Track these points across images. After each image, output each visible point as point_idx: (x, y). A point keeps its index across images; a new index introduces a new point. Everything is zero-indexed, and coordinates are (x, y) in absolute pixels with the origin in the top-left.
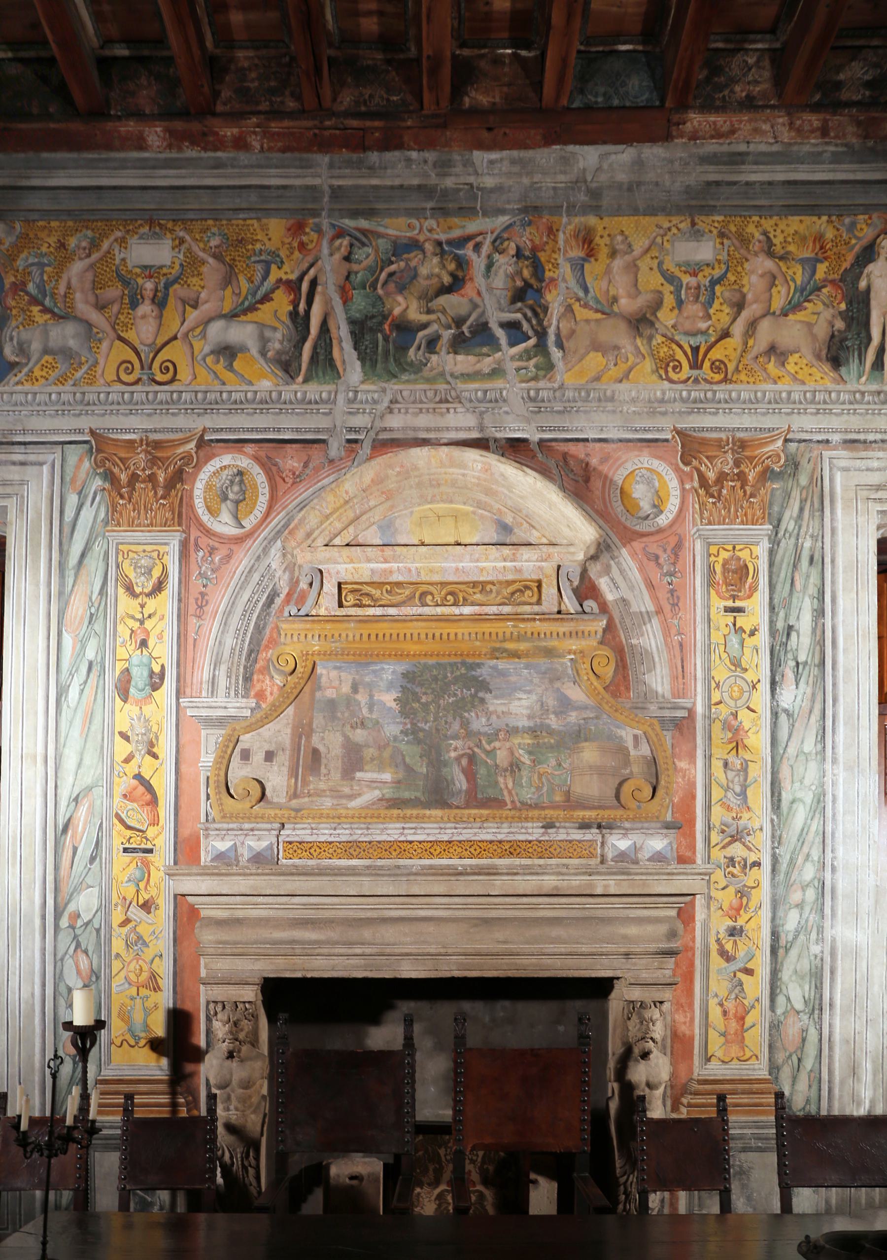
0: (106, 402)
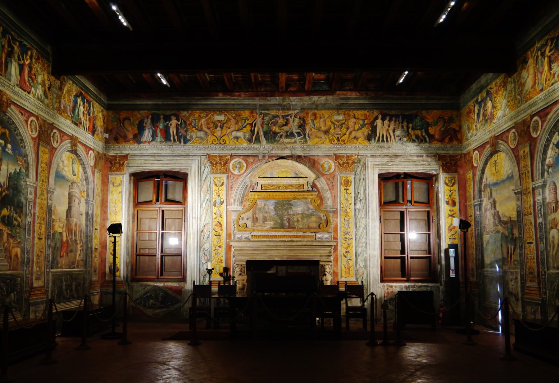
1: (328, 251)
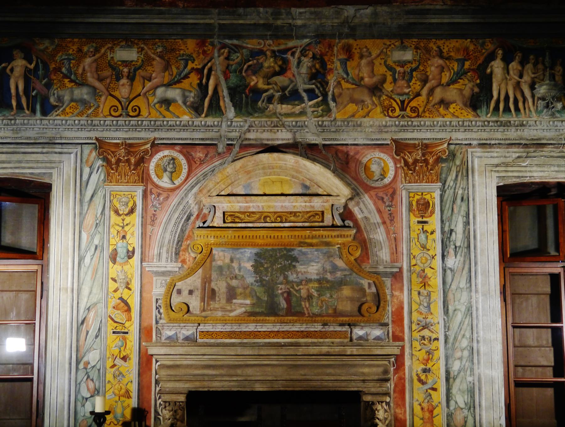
0: (104, 125)
1: (380, 370)
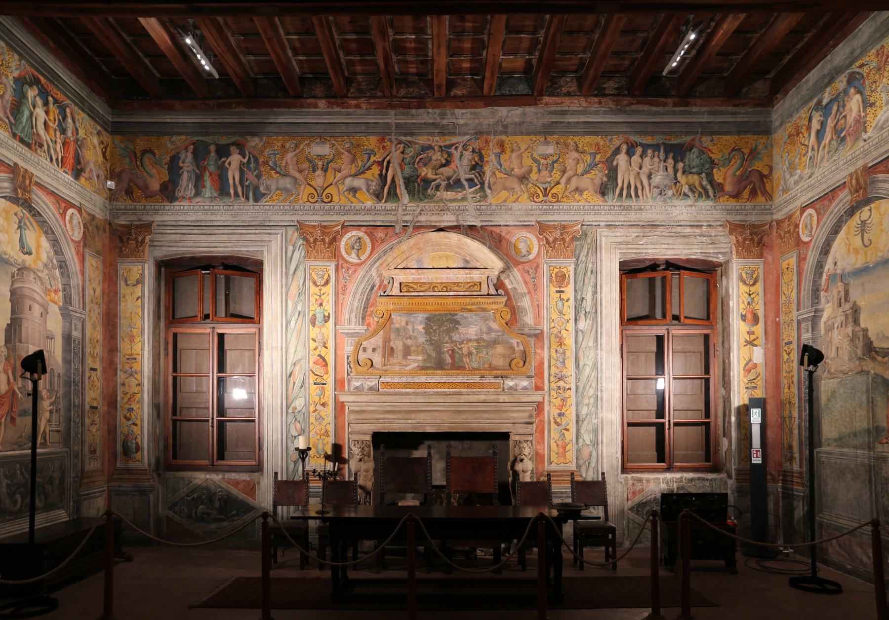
1: (527, 414)
